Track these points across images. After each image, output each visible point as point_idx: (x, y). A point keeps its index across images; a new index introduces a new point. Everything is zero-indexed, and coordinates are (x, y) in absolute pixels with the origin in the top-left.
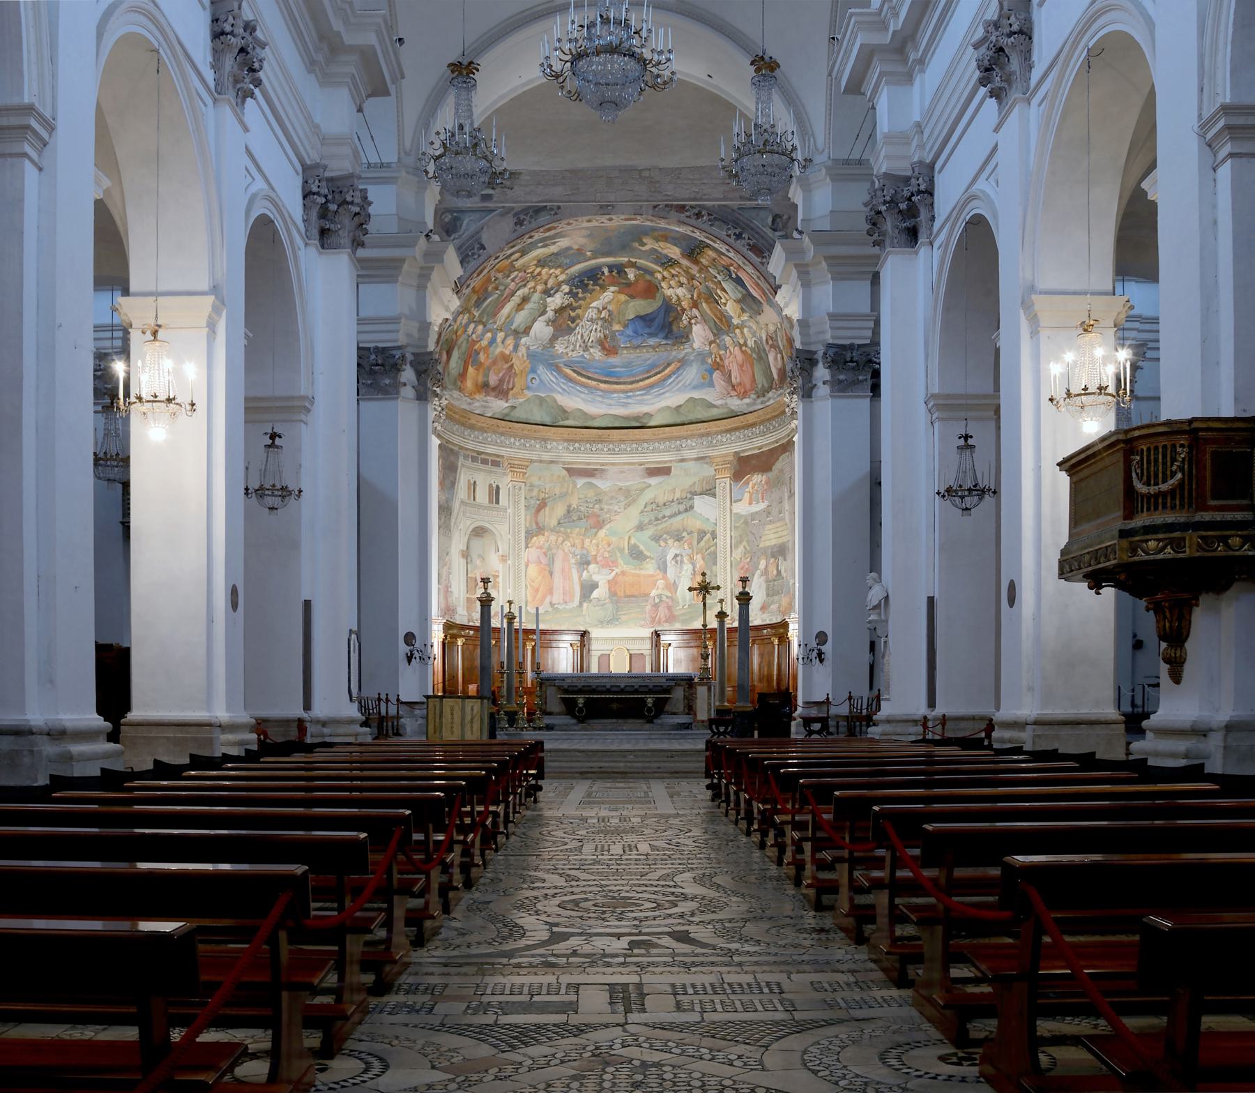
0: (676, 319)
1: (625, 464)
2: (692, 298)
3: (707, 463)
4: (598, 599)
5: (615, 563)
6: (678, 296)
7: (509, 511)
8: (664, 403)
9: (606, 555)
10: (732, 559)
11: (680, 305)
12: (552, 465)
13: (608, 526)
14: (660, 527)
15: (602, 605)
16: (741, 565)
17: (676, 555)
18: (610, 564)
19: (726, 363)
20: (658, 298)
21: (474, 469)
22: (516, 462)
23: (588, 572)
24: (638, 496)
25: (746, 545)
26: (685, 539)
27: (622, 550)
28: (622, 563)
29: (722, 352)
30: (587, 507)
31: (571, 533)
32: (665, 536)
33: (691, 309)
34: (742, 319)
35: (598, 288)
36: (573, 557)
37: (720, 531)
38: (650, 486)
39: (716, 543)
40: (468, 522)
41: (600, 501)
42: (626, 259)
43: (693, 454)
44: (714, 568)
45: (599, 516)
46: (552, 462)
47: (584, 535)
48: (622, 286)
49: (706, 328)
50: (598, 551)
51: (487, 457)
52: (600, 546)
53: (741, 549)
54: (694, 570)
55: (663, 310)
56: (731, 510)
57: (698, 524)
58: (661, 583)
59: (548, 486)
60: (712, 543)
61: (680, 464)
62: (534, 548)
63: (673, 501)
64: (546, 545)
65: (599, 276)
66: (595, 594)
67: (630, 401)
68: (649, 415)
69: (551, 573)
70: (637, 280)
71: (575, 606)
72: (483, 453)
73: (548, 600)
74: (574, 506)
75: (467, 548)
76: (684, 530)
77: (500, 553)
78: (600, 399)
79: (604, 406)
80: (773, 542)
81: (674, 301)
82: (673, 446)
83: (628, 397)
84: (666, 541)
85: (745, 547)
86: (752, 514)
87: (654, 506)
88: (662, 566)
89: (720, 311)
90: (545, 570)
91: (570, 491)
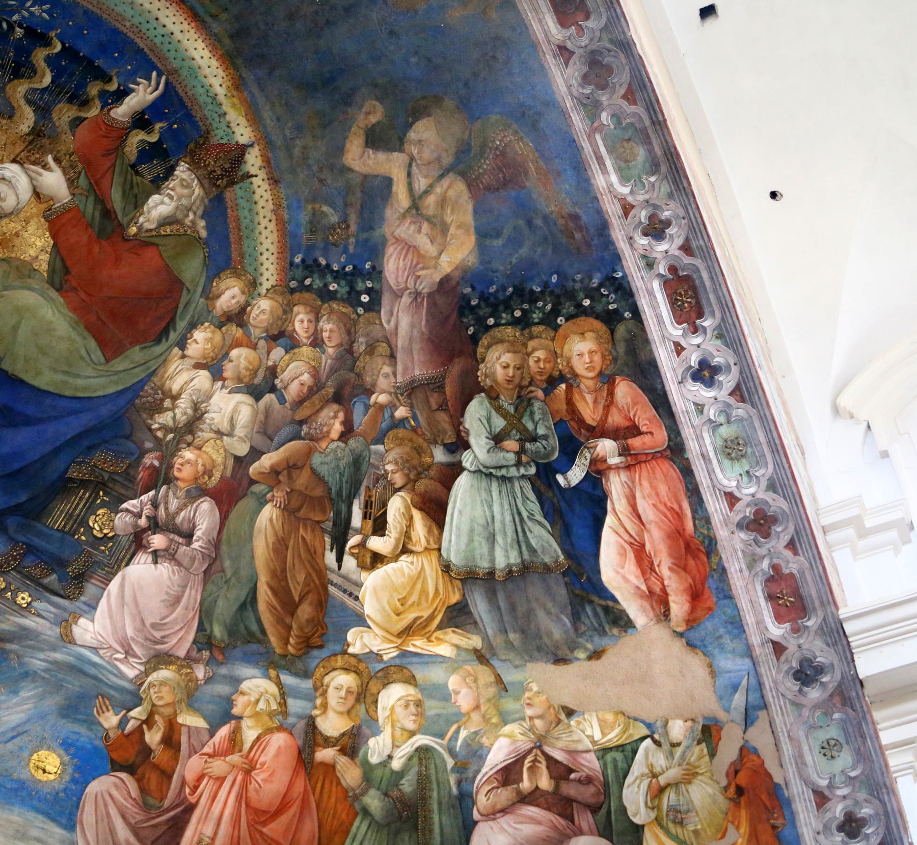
0: (100, 485)
2: (240, 461)
6: (198, 415)
11: (168, 453)
19: (191, 767)
20: (120, 364)
29: (190, 720)
33: (198, 491)
34: (417, 645)
35: (27, 119)
42: (243, 133)
48: (90, 208)
49: (192, 596)
55: (85, 420)
65: (94, 90)
70: (145, 242)
81: (165, 418)
89: (320, 572)
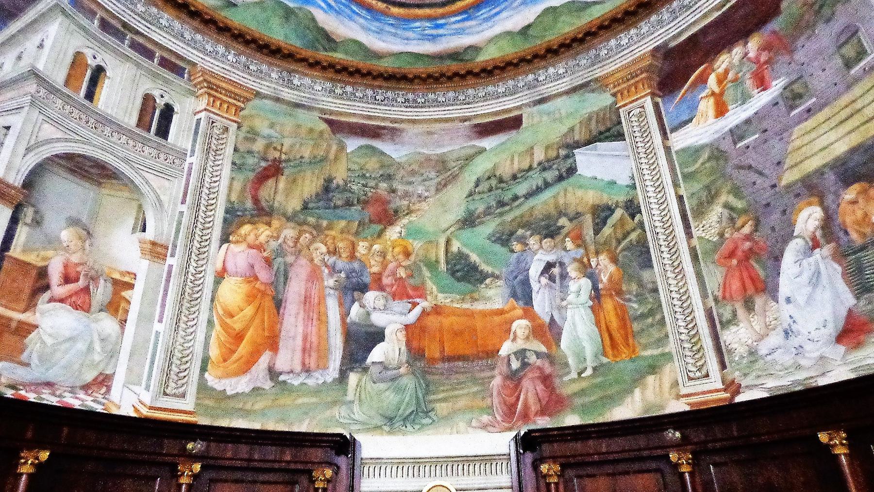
1: (437, 121)
3: (593, 91)
4: (384, 366)
5: (420, 291)
7: (189, 160)
8: (498, 29)
9: (402, 273)
10: (695, 242)
12: (301, 113)
13: (405, 221)
14: (508, 218)
15: (393, 379)
17: (549, 266)
18: (411, 292)
21: (103, 43)
22: (224, 85)
23: (362, 306)
24: (461, 168)
26: (564, 231)
27: (432, 265)
28: (435, 289)
30: (365, 186)
31: (330, 227)
32: (520, 232)
36: (331, 275)
37: (647, 197)
38: (482, 151)
39: (641, 225)
40: (49, 131)
41: (389, 177)
43: (564, 84)
44: (646, 275)
45: (389, 202)
46: (297, 106)
47: (357, 233)
50: (384, 266)
51: (150, 46)
52: (389, 257)
53: (716, 212)
54: (595, 288)
56: (668, 149)
57: (591, 197)
58: (521, 326)
59: (287, 143)
60: (630, 224)
61: (536, 108)
62: (243, 247)
63: (530, 168)
64: (274, 244)
66: (377, 354)
67: (441, 31)
68: (475, 49)
69: (278, 304)
71: (329, 379)
72: (137, 33)
73: (264, 360)
74: (339, 180)
75: (29, 183)
76: (561, 214)
77: (150, 235)
78: (394, 31)
79: (399, 40)
80: (841, 148)
82: (521, 84)
83: (438, 27)
84: (523, 241)
85: (727, 206)
86: (731, 131)
87: (494, 182)
88: (519, 291)
90: (264, 294)
91: (332, 156)
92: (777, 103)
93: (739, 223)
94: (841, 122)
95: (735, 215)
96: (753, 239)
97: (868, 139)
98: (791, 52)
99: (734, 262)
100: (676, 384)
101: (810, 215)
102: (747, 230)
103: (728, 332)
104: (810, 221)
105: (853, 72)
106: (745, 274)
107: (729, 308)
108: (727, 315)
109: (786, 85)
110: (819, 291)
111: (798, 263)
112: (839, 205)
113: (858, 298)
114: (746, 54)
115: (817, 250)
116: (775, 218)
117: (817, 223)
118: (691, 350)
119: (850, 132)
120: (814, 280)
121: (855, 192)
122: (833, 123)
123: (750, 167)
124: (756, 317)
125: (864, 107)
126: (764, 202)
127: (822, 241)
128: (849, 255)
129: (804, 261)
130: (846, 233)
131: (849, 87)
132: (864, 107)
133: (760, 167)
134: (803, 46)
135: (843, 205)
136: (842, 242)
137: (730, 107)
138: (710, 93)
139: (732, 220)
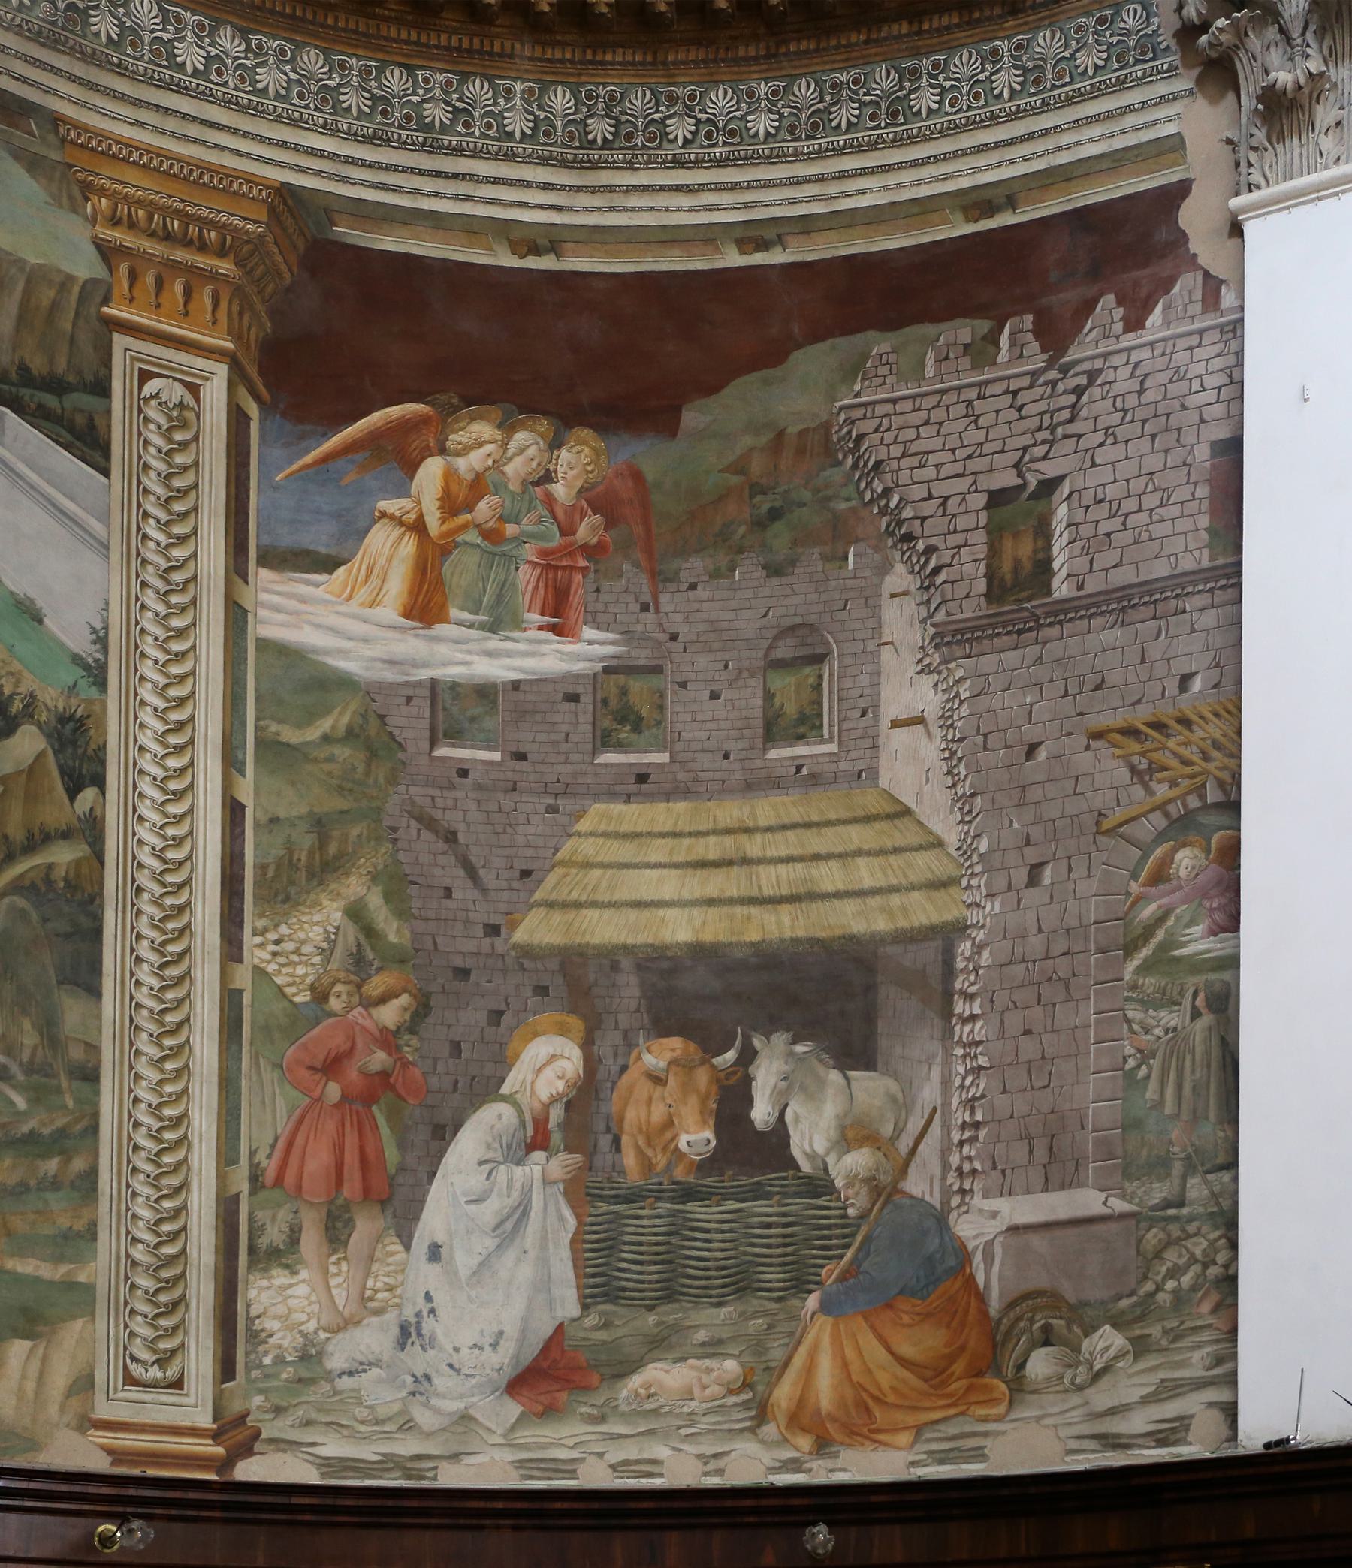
16: (324, 1037)
25: (375, 900)
85: (355, 913)
86: (434, 683)
92: (574, 698)
93: (377, 984)
94: (703, 864)
95: (370, 955)
96: (398, 1048)
97: (740, 945)
98: (660, 578)
99: (333, 1091)
100: (84, 1384)
101: (553, 1058)
102: (389, 1014)
103: (265, 1283)
104: (549, 1073)
105: (773, 754)
106: (351, 1141)
107: (284, 1215)
108: (274, 1235)
109: (614, 663)
110: (510, 1255)
111: (487, 1167)
112: (624, 1069)
113: (585, 1307)
114: (548, 477)
115: (539, 1156)
116: (472, 1018)
117: (560, 1086)
118: (151, 1298)
119: (711, 902)
120: (509, 1225)
121: (669, 1056)
122: (684, 849)
123: (451, 837)
124: (344, 1266)
125: (761, 861)
126: (458, 962)
127: (556, 1138)
128: (602, 1198)
129: (502, 1167)
130: (617, 1142)
131: (750, 787)
132: (761, 861)
133: (476, 856)
134: (693, 587)
135: (633, 1074)
136: (598, 1161)
137: (454, 613)
138: (411, 517)
139: (358, 961)
